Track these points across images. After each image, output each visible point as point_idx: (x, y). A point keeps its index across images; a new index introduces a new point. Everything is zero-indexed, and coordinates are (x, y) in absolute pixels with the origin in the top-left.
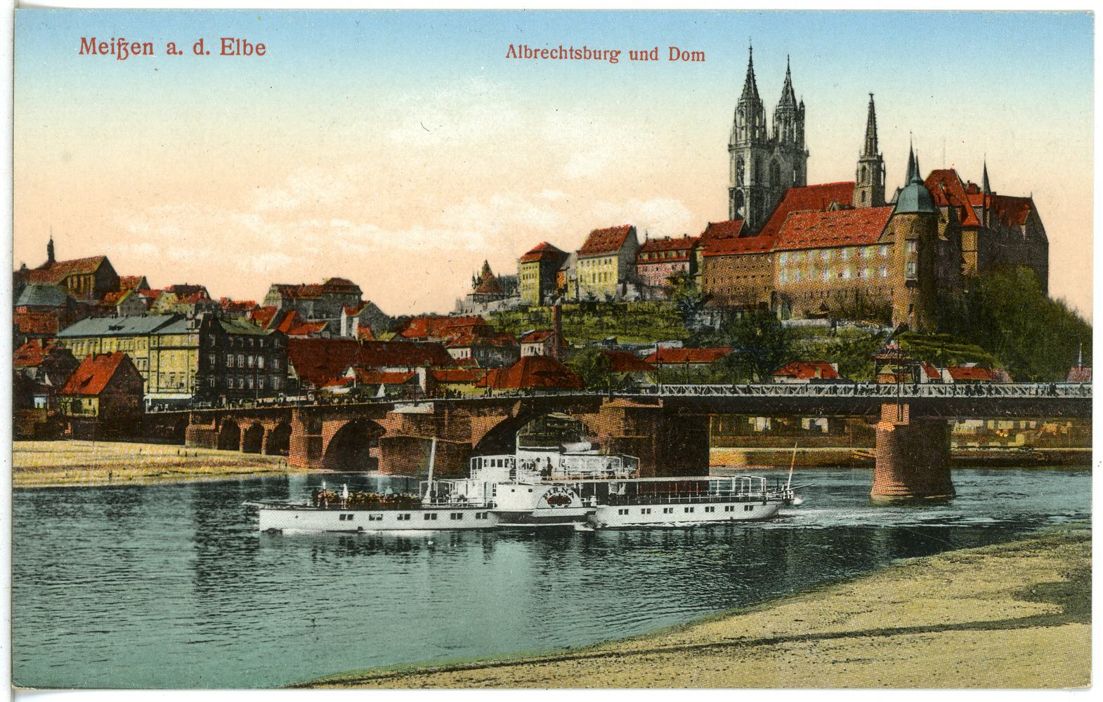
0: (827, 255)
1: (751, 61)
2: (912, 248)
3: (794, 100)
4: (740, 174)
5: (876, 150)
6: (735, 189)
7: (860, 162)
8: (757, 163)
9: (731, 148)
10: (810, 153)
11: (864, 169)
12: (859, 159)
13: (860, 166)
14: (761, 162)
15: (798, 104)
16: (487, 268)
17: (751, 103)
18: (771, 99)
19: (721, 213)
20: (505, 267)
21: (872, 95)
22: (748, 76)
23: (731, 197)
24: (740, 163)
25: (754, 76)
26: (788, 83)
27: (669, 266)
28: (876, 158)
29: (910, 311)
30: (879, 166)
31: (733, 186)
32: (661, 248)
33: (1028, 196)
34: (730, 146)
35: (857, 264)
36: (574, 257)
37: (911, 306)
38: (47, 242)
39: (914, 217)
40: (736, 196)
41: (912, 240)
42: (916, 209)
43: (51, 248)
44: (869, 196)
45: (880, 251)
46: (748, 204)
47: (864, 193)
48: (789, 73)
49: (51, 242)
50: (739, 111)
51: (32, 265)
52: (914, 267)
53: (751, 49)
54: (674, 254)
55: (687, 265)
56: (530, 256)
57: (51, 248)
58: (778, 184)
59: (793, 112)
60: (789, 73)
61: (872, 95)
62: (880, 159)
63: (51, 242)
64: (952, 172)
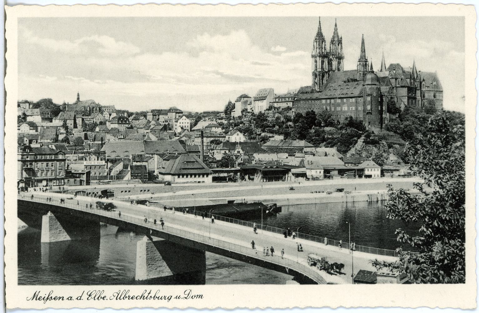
1: (320, 22)
2: (369, 99)
3: (338, 36)
5: (365, 57)
6: (314, 72)
7: (359, 61)
8: (323, 62)
9: (313, 56)
11: (360, 64)
12: (358, 61)
13: (359, 63)
14: (324, 62)
17: (320, 37)
18: (328, 35)
19: (308, 81)
20: (233, 102)
24: (316, 61)
26: (336, 30)
28: (364, 60)
29: (369, 124)
30: (366, 64)
32: (281, 98)
34: (312, 55)
36: (253, 99)
37: (369, 123)
38: (77, 94)
39: (370, 86)
40: (315, 75)
41: (369, 95)
42: (370, 83)
43: (78, 95)
44: (362, 75)
46: (318, 78)
47: (360, 74)
48: (336, 25)
49: (78, 94)
52: (369, 107)
54: (287, 99)
55: (291, 103)
57: (78, 95)
59: (337, 41)
60: (336, 25)
62: (366, 61)
63: (78, 94)
64: (398, 64)
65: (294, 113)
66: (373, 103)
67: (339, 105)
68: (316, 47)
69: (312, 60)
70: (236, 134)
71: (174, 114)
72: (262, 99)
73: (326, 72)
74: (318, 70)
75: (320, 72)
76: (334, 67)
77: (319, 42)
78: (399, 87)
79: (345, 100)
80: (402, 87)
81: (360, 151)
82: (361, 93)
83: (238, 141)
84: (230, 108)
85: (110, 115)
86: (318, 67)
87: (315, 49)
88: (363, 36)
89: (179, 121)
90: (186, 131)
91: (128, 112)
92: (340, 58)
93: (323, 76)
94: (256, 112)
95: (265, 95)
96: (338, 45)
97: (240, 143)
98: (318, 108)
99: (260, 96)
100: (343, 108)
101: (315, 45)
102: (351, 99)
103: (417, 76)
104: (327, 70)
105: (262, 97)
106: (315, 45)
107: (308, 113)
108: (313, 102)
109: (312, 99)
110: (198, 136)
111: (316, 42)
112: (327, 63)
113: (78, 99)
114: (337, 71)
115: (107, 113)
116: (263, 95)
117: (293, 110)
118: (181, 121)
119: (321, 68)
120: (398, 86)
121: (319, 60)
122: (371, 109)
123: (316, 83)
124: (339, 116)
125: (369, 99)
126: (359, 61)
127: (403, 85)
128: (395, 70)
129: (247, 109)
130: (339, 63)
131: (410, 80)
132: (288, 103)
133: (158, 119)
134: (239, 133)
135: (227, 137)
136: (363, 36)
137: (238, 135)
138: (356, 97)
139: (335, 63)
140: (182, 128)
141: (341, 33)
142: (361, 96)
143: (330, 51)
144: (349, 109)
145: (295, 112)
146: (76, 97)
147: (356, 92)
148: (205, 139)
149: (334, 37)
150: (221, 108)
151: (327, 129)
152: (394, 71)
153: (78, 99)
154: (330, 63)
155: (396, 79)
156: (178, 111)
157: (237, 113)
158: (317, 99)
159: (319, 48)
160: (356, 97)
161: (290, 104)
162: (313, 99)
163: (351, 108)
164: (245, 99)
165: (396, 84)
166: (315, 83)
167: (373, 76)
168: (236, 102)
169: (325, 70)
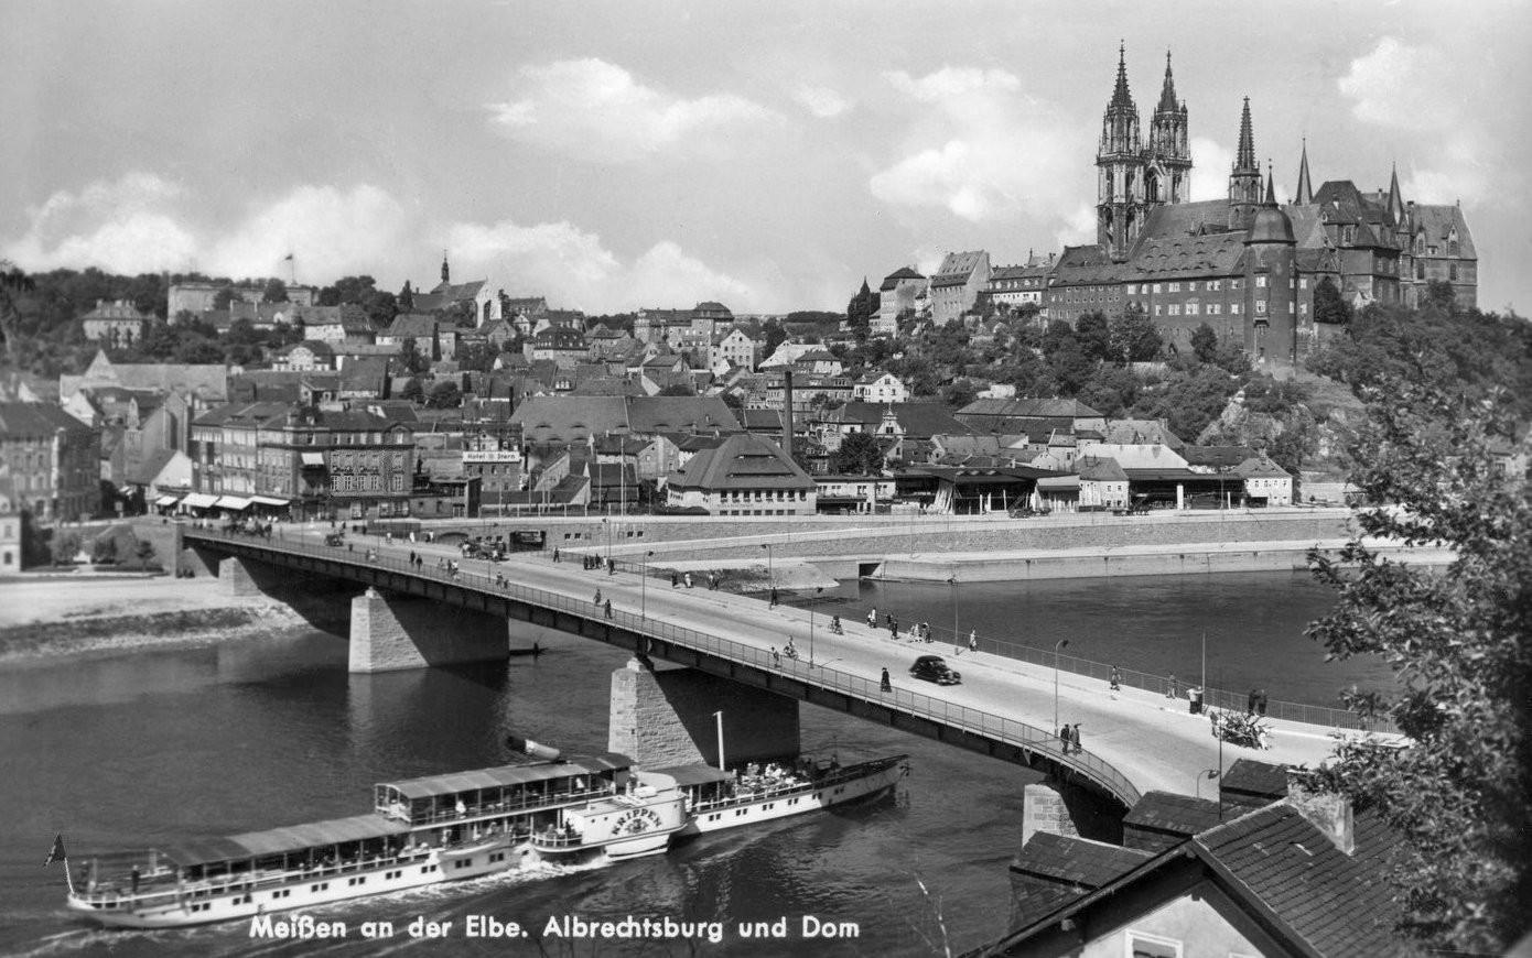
0: (1173, 288)
1: (1122, 64)
3: (1174, 106)
4: (1110, 189)
5: (1252, 162)
7: (1234, 176)
8: (1129, 179)
9: (1100, 162)
10: (1194, 164)
11: (1237, 183)
14: (1133, 177)
15: (1181, 105)
16: (865, 288)
17: (1121, 107)
18: (1146, 102)
20: (874, 288)
21: (1246, 99)
22: (1118, 81)
23: (1101, 215)
24: (1110, 176)
25: (1125, 80)
27: (1021, 294)
30: (1254, 182)
31: (1101, 203)
32: (1009, 277)
33: (1454, 204)
34: (1098, 159)
35: (1204, 299)
36: (930, 282)
39: (1266, 246)
40: (1106, 213)
41: (1262, 272)
42: (1265, 236)
43: (445, 268)
45: (1230, 284)
48: (1169, 73)
50: (1109, 117)
51: (426, 290)
53: (1122, 51)
54: (1027, 283)
55: (1039, 294)
56: (889, 283)
57: (445, 268)
58: (1155, 199)
59: (1172, 115)
60: (1169, 73)
61: (1246, 99)
62: (1256, 174)
64: (1348, 184)
65: (1046, 322)
66: (1272, 294)
67: (1174, 299)
68: (1109, 136)
69: (1095, 174)
70: (883, 379)
71: (710, 322)
72: (958, 281)
73: (1139, 207)
74: (1115, 201)
75: (1120, 205)
76: (1161, 192)
77: (1120, 120)
78: (1349, 248)
79: (1192, 286)
80: (1356, 248)
81: (1232, 430)
82: (1240, 265)
83: (887, 399)
84: (865, 305)
85: (533, 324)
86: (1116, 193)
87: (1109, 141)
88: (1246, 104)
89: (723, 344)
90: (743, 371)
91: (579, 315)
92: (1181, 166)
93: (1130, 218)
94: (940, 321)
95: (965, 272)
96: (1175, 130)
97: (895, 405)
98: (1111, 305)
99: (951, 273)
100: (1188, 306)
101: (1109, 131)
102: (1209, 284)
103: (1402, 218)
104: (1141, 201)
105: (956, 277)
106: (1109, 131)
107: (1085, 324)
108: (1101, 290)
109: (1096, 284)
110: (776, 384)
111: (1112, 121)
112: (1142, 182)
113: (446, 277)
114: (1170, 203)
115: (525, 320)
116: (958, 272)
117: (1044, 314)
118: (727, 342)
119: (1123, 193)
120: (1345, 244)
121: (1120, 175)
122: (1268, 313)
123: (1111, 238)
124: (1175, 332)
125: (1261, 282)
126: (1234, 176)
127: (1361, 243)
128: (1336, 199)
129: (914, 311)
130: (1176, 180)
131: (1382, 229)
132: (1031, 294)
133: (666, 337)
134: (889, 376)
135: (857, 387)
136: (1246, 104)
137: (888, 382)
138: (1226, 277)
139: (1163, 181)
140: (731, 363)
141: (1179, 98)
142: (1240, 271)
143: (1151, 146)
144: (1203, 309)
145: (1049, 320)
146: (439, 273)
147: (1226, 264)
148: (794, 392)
149: (1162, 107)
150: (840, 306)
151: (1141, 367)
152: (1336, 204)
153: (446, 277)
154: (1150, 176)
155: (1341, 225)
156: (722, 316)
157: (885, 322)
158: (1112, 283)
159: (1121, 140)
160: (1226, 277)
161: (1033, 297)
162: (1102, 284)
163: (1209, 307)
164: (909, 282)
165: (1340, 240)
166: (1105, 237)
167: (1274, 217)
168: (883, 289)
169: (1136, 200)
